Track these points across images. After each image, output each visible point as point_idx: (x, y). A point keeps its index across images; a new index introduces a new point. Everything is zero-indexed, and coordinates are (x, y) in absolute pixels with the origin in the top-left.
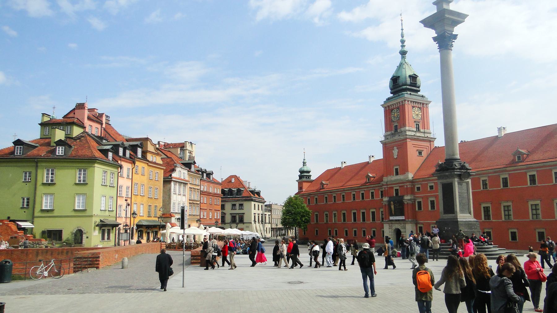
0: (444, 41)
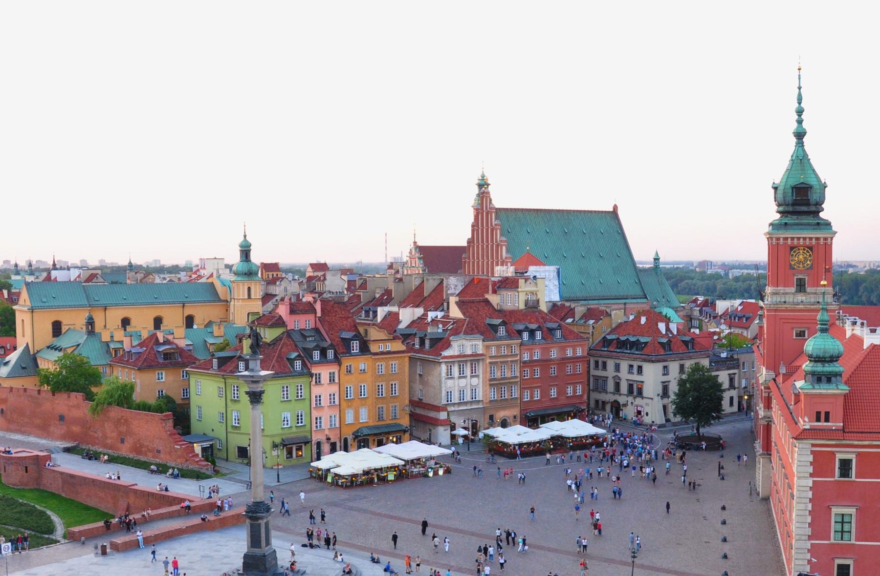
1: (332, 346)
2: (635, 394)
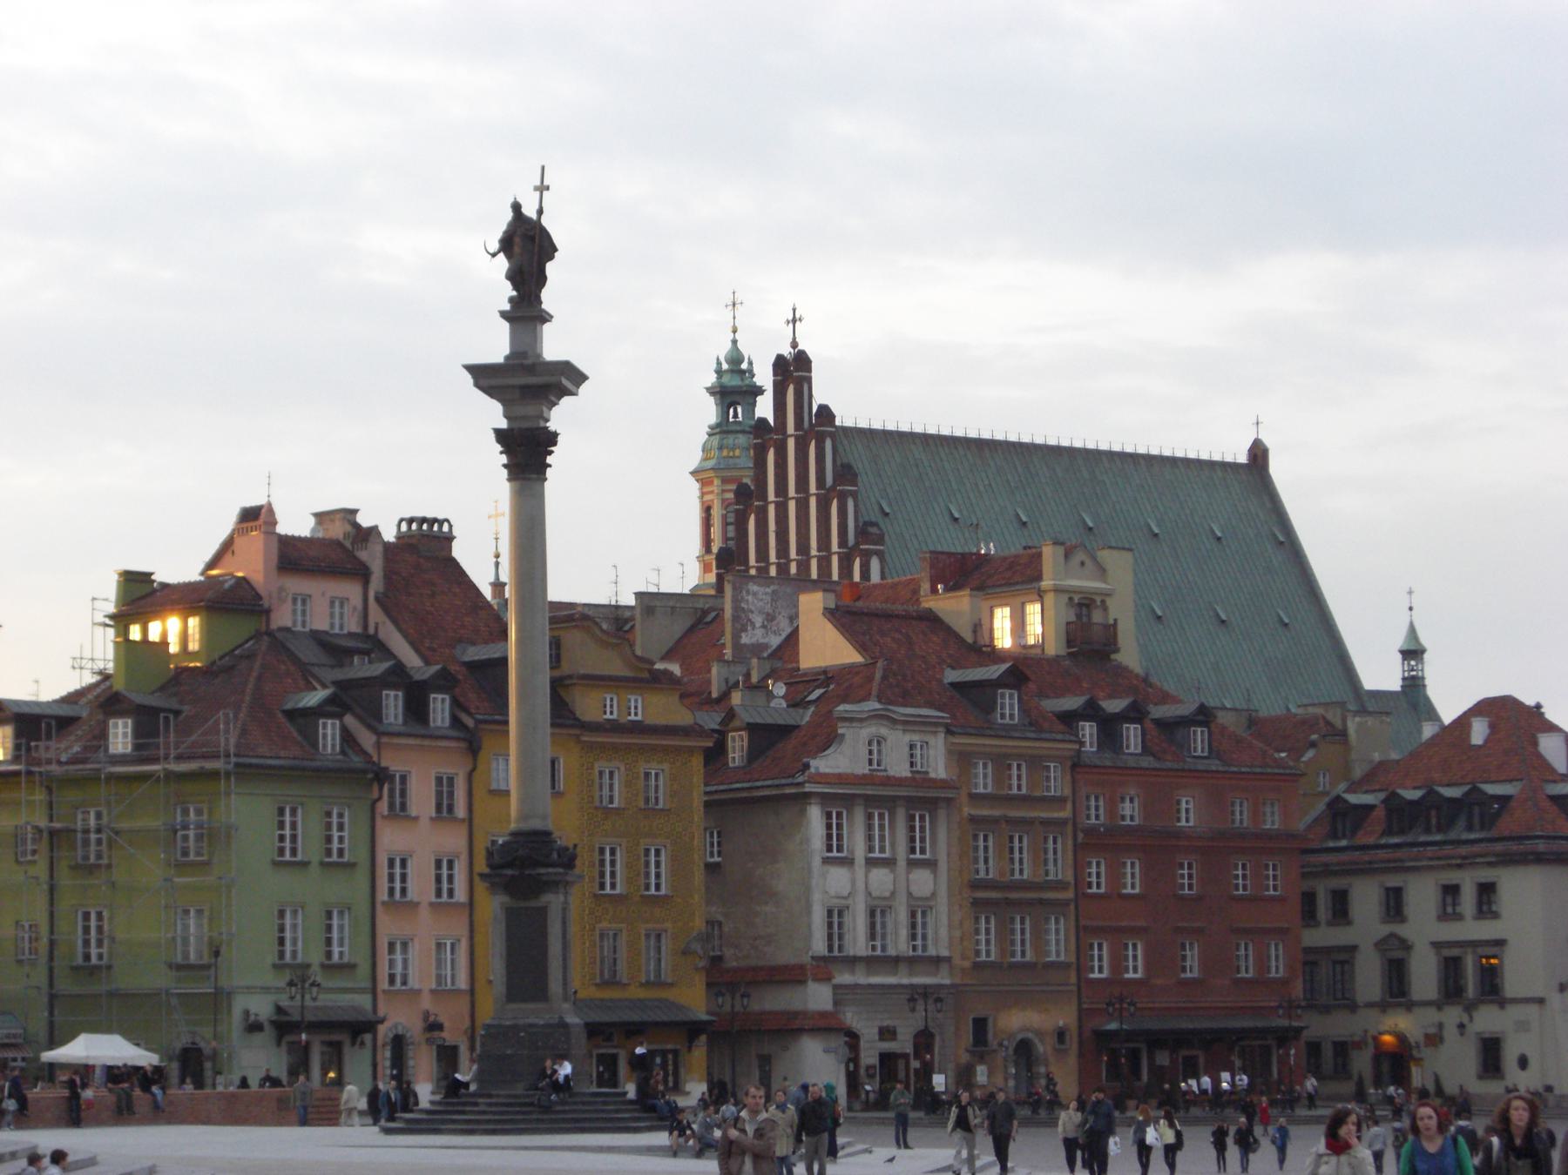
0: (527, 451)
1: (444, 680)
2: (1471, 990)
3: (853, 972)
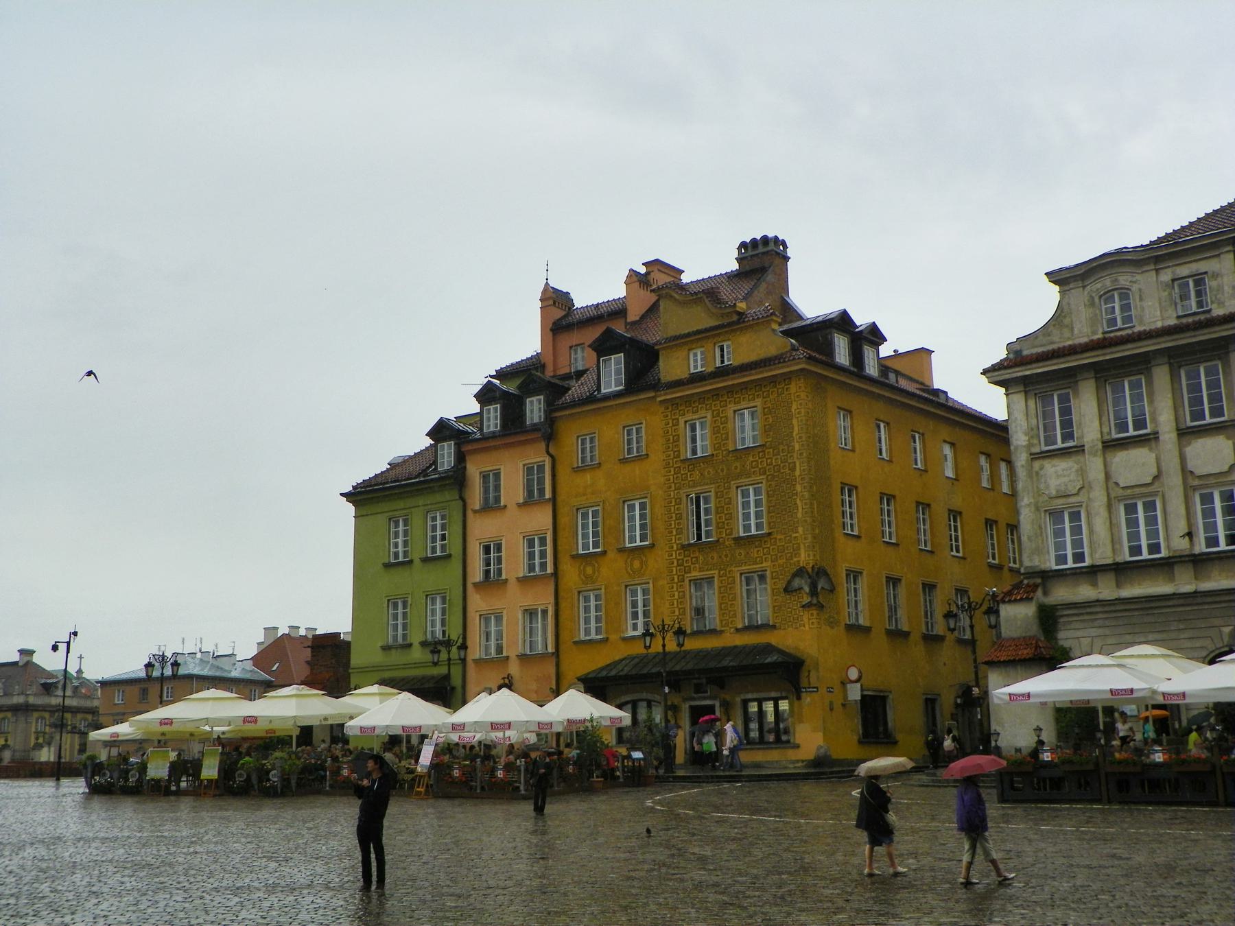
3: (1094, 584)
